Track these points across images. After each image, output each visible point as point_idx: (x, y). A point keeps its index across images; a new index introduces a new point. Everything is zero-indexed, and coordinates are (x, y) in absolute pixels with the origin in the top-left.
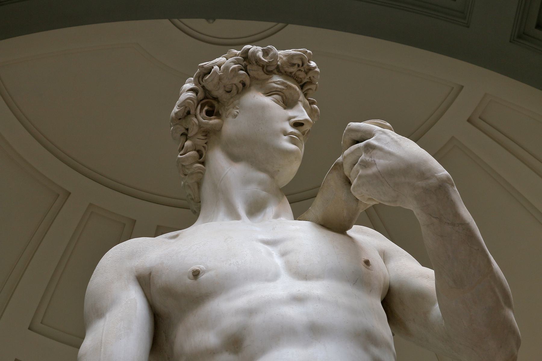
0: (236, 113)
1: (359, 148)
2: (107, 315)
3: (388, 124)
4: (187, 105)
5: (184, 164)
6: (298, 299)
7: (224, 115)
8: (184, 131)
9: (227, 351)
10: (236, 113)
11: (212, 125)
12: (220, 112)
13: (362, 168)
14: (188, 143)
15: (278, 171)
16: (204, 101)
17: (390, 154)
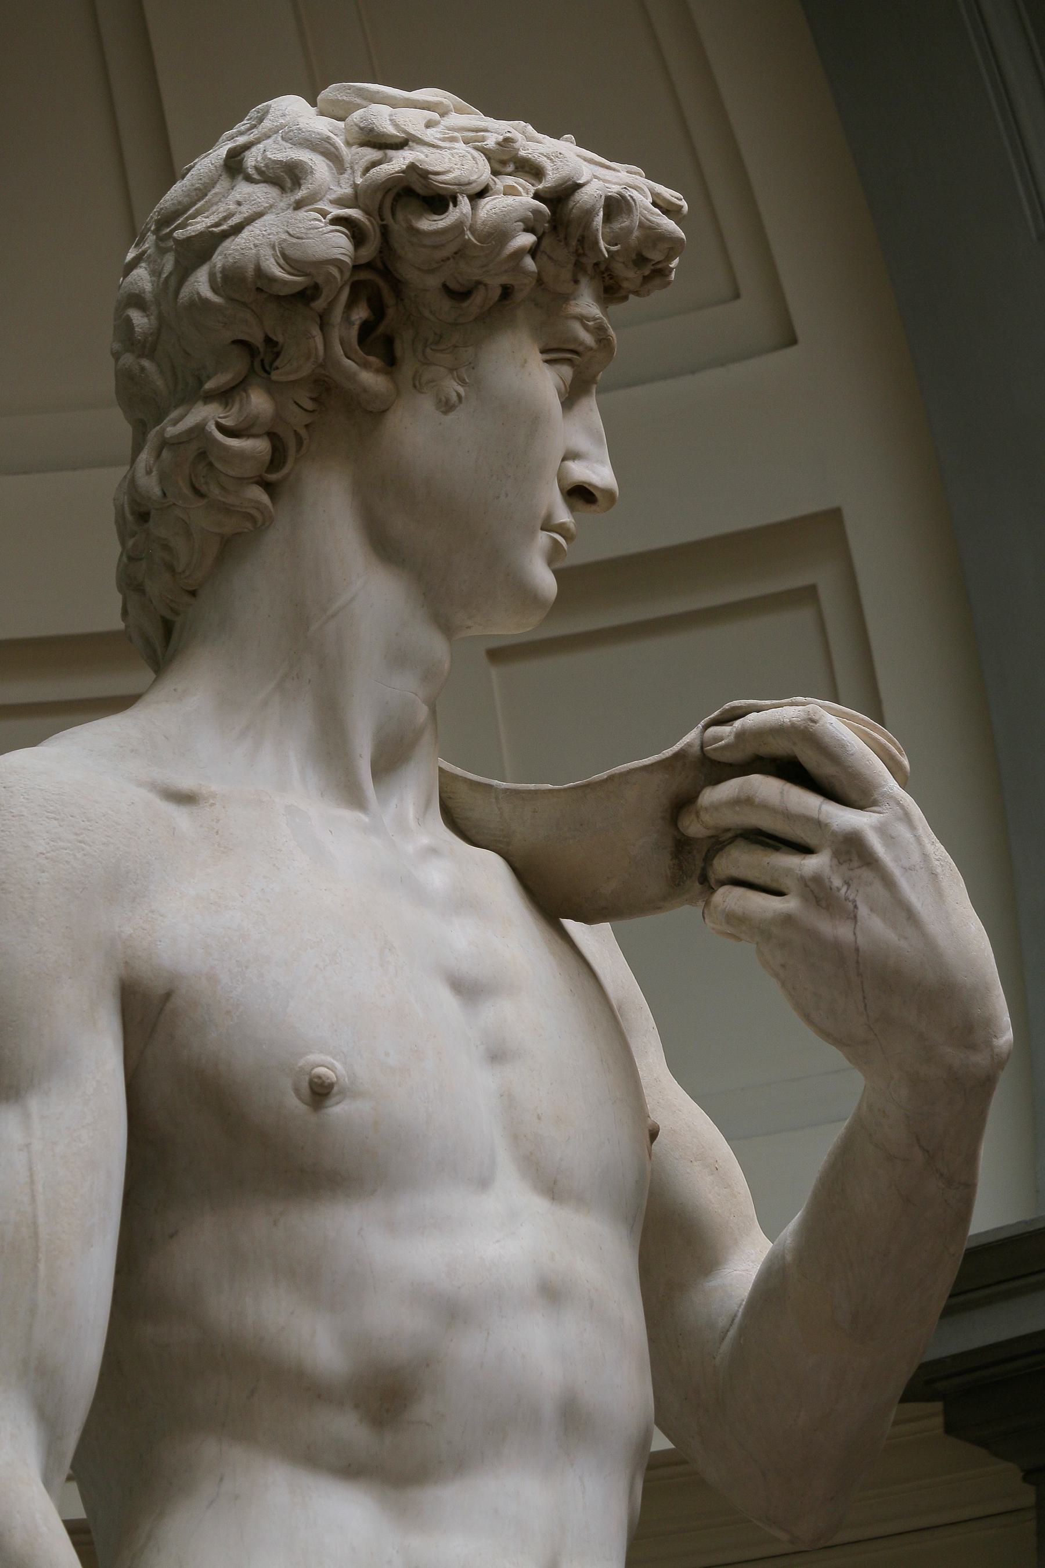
0: (454, 398)
1: (819, 825)
2: (34, 1104)
3: (906, 762)
4: (320, 280)
5: (218, 465)
6: (552, 1293)
7: (407, 369)
8: (256, 337)
9: (356, 1406)
10: (454, 398)
11: (365, 390)
12: (398, 353)
13: (804, 898)
14: (258, 402)
15: (469, 627)
16: (364, 275)
17: (910, 915)
